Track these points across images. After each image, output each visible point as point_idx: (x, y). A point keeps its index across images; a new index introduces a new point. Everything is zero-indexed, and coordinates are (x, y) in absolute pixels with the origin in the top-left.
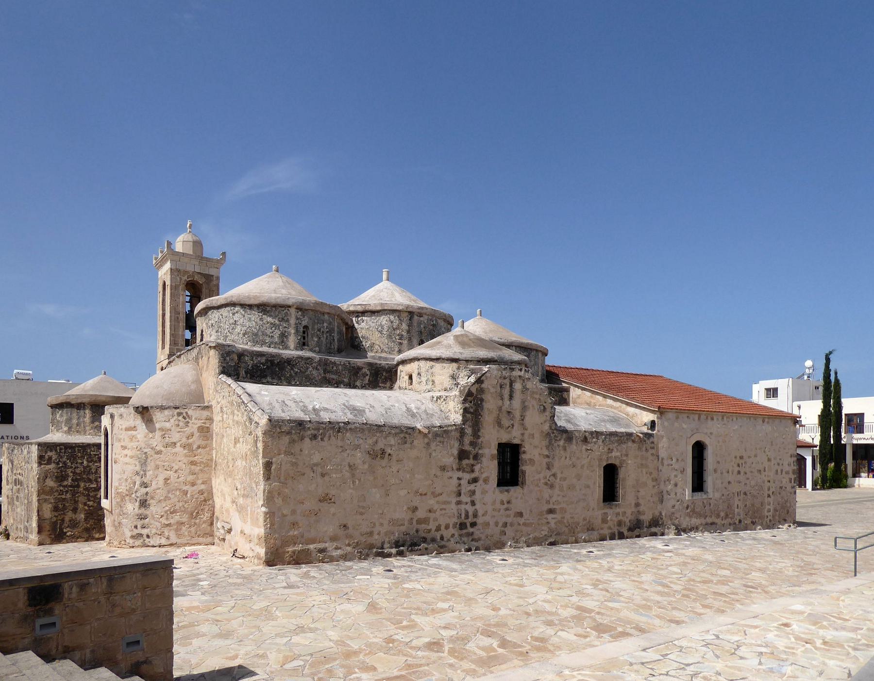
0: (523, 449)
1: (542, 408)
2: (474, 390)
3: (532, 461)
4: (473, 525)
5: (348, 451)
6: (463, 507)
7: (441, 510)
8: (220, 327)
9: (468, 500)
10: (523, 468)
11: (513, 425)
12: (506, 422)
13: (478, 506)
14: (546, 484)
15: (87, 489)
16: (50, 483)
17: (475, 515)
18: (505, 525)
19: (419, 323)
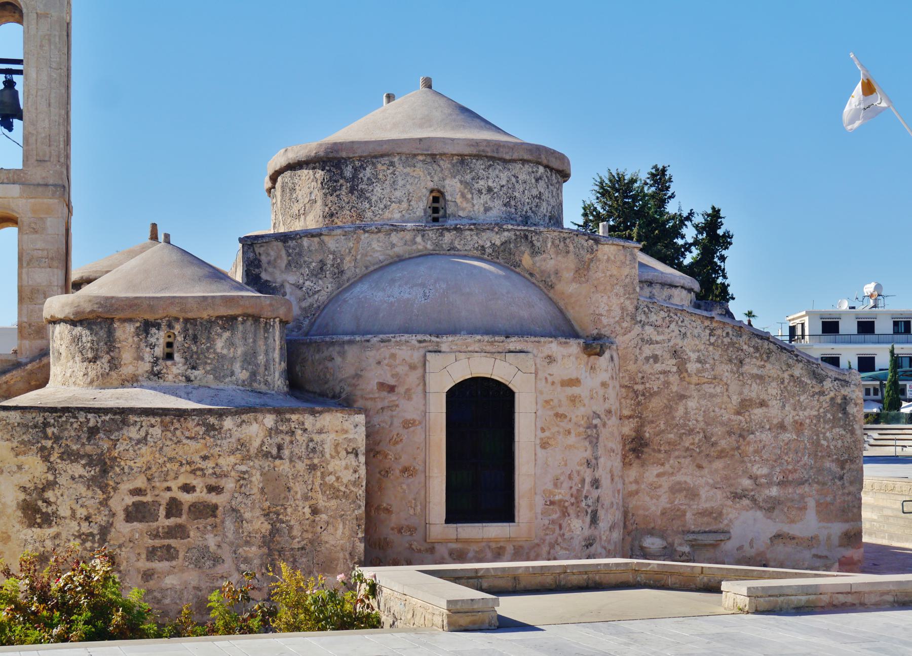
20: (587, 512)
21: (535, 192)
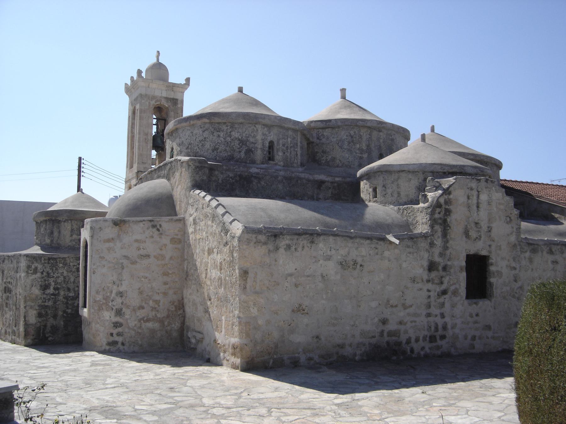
0: (490, 261)
1: (508, 219)
2: (442, 200)
3: (500, 274)
4: (443, 337)
5: (321, 262)
6: (431, 319)
7: (411, 322)
8: (190, 144)
9: (438, 312)
10: (492, 280)
11: (480, 236)
12: (473, 234)
13: (447, 319)
14: (514, 296)
15: (66, 298)
16: (36, 291)
17: (445, 328)
18: (474, 338)
19: (378, 139)
20: (113, 309)
21: (201, 138)
